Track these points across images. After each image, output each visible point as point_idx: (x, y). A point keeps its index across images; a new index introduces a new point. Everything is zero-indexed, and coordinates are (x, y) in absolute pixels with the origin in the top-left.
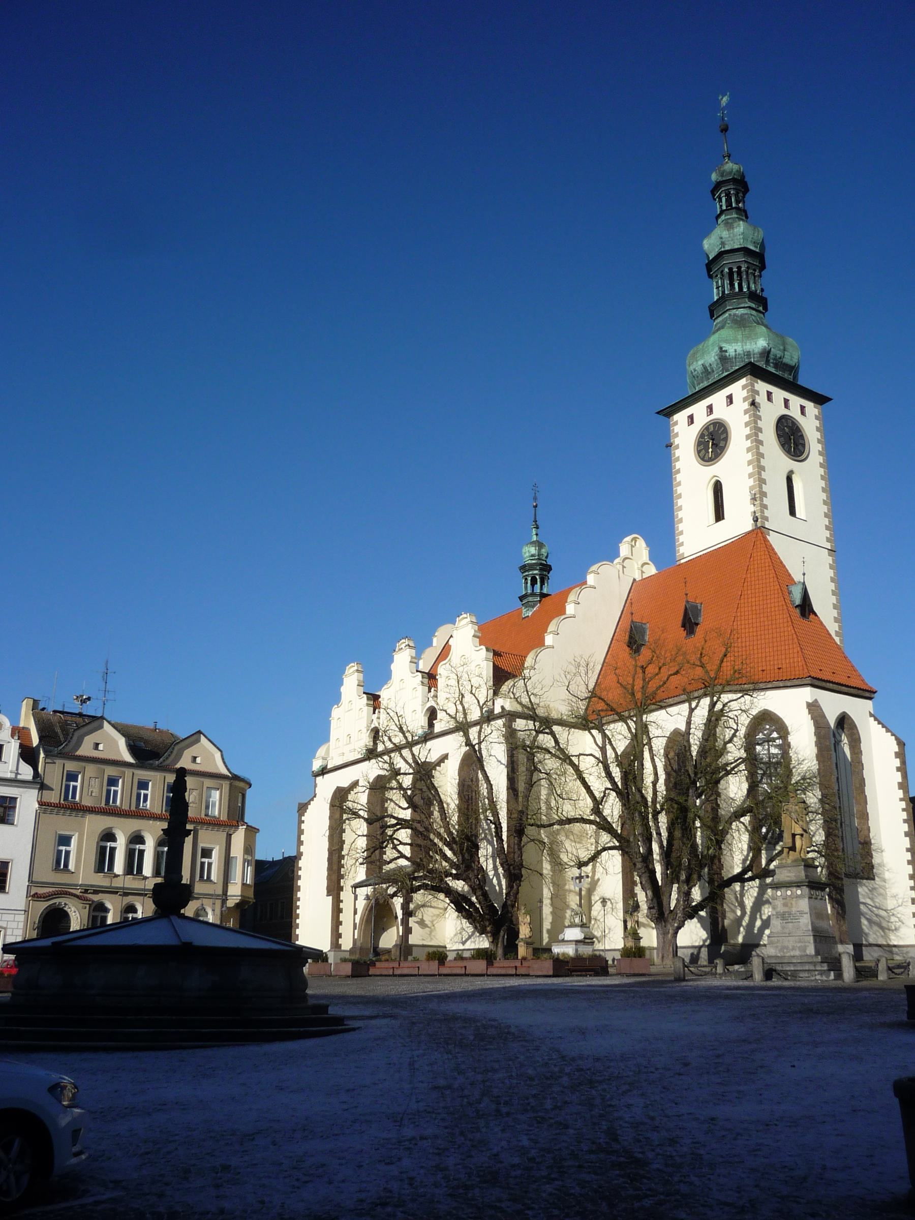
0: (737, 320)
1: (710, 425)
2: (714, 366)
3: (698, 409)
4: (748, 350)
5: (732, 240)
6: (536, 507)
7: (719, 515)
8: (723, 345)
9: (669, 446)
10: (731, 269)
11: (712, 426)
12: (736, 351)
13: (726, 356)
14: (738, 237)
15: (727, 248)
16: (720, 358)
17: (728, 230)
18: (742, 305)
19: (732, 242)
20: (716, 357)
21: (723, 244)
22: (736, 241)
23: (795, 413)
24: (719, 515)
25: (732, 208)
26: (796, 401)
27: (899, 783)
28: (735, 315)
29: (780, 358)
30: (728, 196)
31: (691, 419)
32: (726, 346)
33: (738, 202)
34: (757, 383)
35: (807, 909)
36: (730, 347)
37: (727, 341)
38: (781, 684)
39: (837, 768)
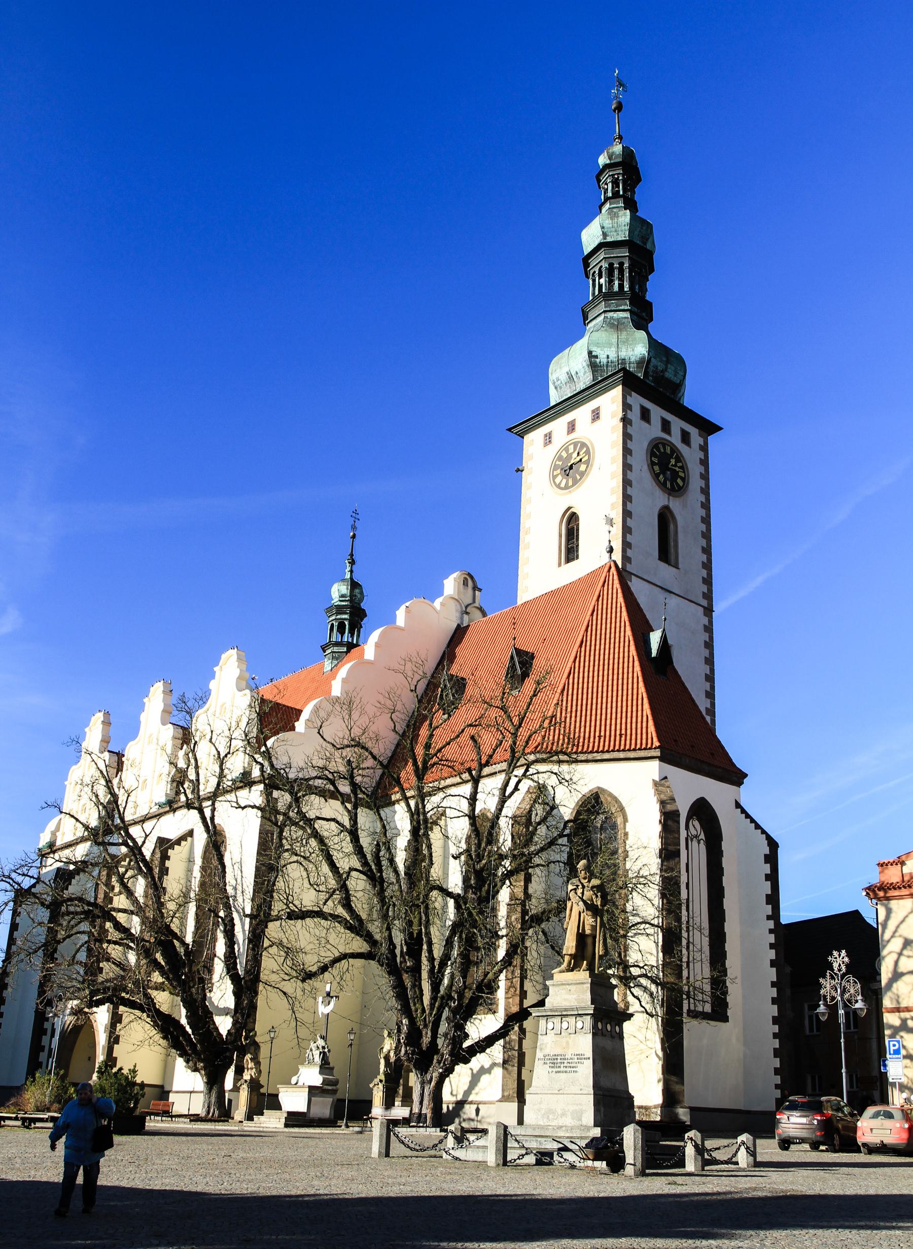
0: (613, 324)
1: (570, 445)
2: (581, 374)
3: (558, 426)
4: (623, 357)
5: (616, 231)
7: (571, 552)
8: (593, 349)
9: (519, 471)
10: (611, 265)
11: (572, 446)
12: (608, 357)
13: (595, 362)
14: (623, 228)
15: (609, 239)
17: (612, 219)
18: (622, 308)
19: (615, 234)
21: (605, 235)
22: (620, 233)
23: (675, 439)
24: (571, 552)
25: (620, 196)
26: (677, 424)
27: (767, 895)
28: (612, 318)
29: (662, 371)
30: (615, 183)
31: (548, 438)
32: (597, 351)
33: (624, 190)
34: (631, 396)
35: (589, 1053)
36: (602, 352)
37: (597, 345)
38: (622, 755)
39: (687, 871)
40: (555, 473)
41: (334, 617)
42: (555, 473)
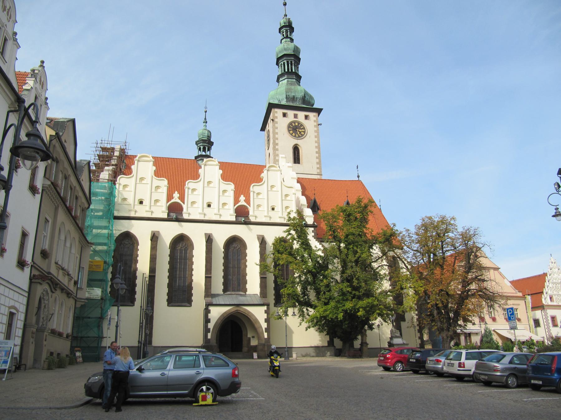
6: (206, 112)
16: (302, 98)
20: (301, 97)
21: (294, 51)
32: (306, 96)
40: (289, 129)
41: (201, 144)
42: (289, 129)
